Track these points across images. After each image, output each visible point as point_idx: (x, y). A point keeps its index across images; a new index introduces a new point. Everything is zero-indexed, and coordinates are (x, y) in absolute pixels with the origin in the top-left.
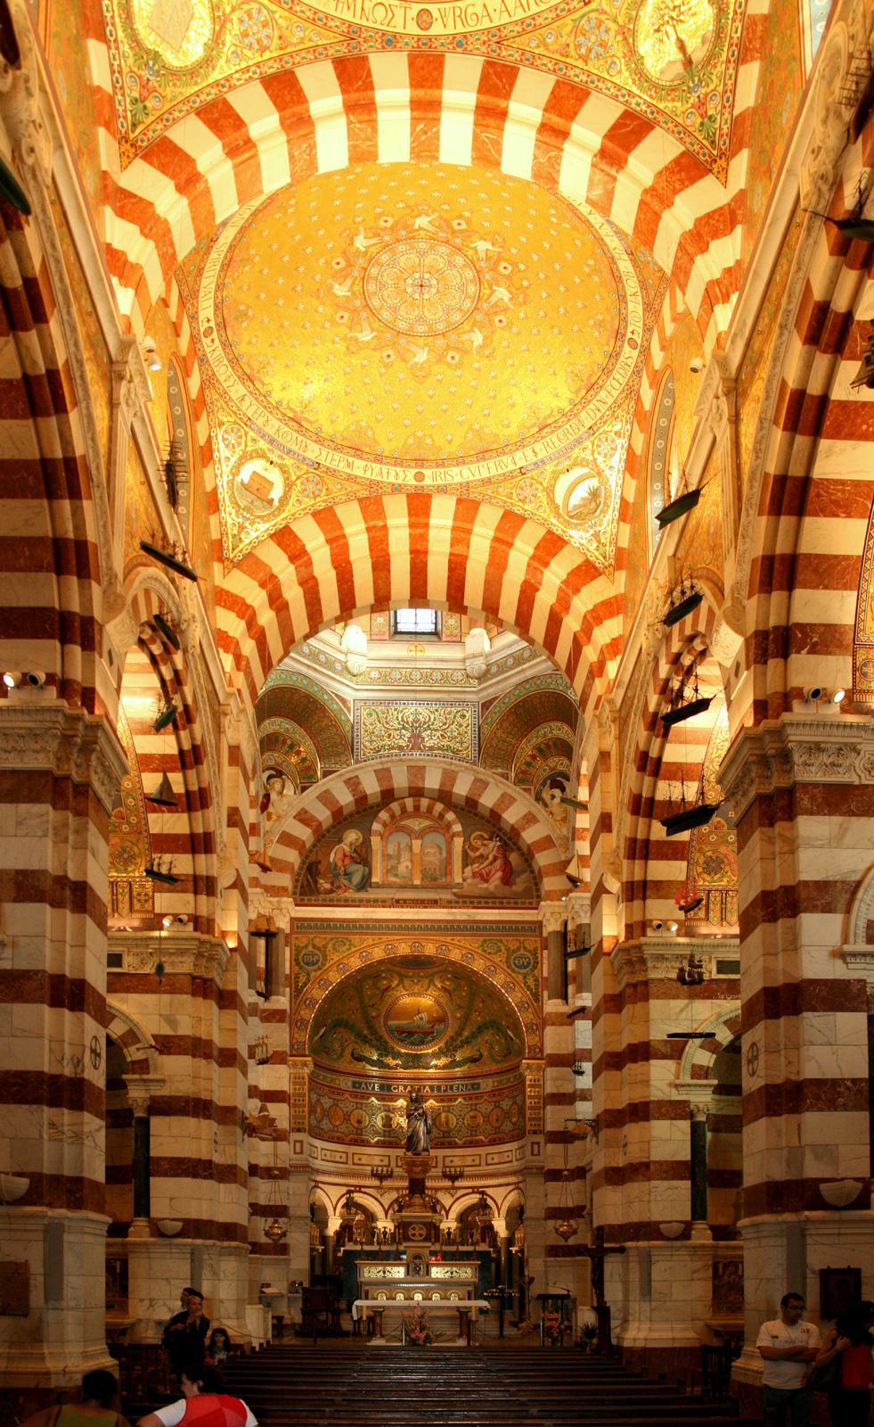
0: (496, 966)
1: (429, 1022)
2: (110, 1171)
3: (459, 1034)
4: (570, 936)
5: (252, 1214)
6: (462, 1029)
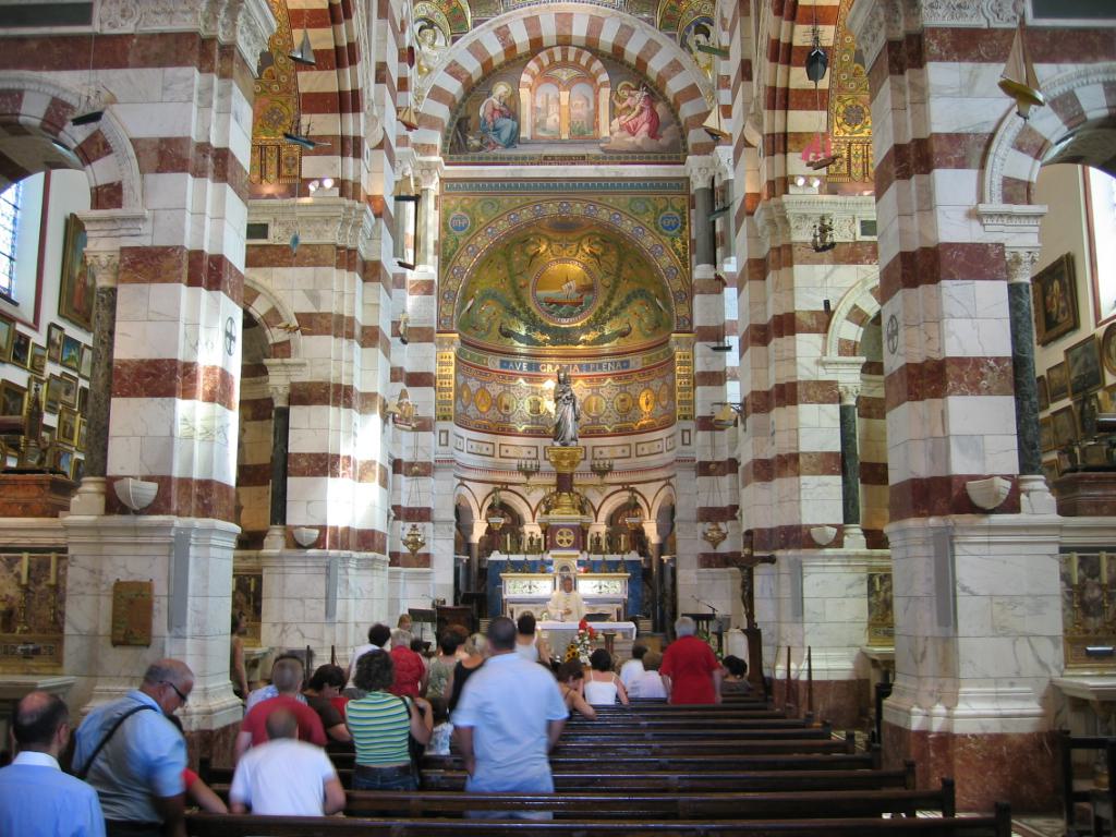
0: (642, 226)
1: (577, 291)
2: (243, 470)
3: (607, 304)
4: (717, 192)
5: (395, 519)
6: (611, 298)
